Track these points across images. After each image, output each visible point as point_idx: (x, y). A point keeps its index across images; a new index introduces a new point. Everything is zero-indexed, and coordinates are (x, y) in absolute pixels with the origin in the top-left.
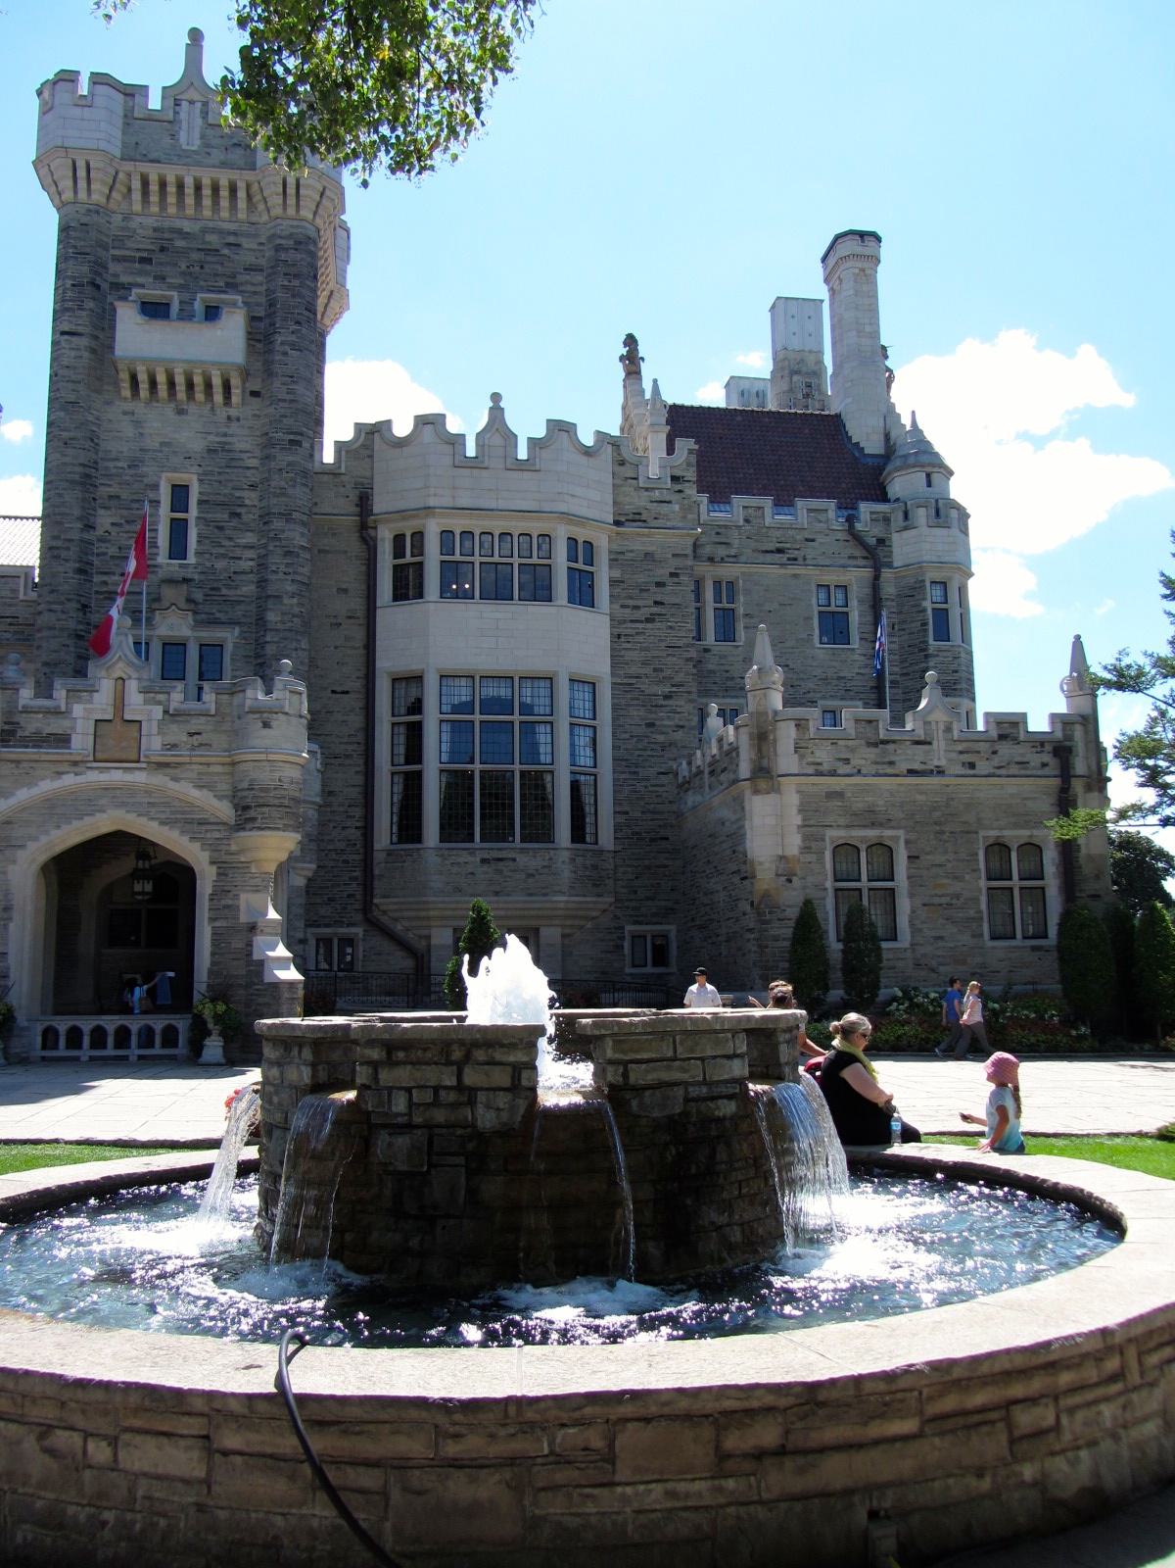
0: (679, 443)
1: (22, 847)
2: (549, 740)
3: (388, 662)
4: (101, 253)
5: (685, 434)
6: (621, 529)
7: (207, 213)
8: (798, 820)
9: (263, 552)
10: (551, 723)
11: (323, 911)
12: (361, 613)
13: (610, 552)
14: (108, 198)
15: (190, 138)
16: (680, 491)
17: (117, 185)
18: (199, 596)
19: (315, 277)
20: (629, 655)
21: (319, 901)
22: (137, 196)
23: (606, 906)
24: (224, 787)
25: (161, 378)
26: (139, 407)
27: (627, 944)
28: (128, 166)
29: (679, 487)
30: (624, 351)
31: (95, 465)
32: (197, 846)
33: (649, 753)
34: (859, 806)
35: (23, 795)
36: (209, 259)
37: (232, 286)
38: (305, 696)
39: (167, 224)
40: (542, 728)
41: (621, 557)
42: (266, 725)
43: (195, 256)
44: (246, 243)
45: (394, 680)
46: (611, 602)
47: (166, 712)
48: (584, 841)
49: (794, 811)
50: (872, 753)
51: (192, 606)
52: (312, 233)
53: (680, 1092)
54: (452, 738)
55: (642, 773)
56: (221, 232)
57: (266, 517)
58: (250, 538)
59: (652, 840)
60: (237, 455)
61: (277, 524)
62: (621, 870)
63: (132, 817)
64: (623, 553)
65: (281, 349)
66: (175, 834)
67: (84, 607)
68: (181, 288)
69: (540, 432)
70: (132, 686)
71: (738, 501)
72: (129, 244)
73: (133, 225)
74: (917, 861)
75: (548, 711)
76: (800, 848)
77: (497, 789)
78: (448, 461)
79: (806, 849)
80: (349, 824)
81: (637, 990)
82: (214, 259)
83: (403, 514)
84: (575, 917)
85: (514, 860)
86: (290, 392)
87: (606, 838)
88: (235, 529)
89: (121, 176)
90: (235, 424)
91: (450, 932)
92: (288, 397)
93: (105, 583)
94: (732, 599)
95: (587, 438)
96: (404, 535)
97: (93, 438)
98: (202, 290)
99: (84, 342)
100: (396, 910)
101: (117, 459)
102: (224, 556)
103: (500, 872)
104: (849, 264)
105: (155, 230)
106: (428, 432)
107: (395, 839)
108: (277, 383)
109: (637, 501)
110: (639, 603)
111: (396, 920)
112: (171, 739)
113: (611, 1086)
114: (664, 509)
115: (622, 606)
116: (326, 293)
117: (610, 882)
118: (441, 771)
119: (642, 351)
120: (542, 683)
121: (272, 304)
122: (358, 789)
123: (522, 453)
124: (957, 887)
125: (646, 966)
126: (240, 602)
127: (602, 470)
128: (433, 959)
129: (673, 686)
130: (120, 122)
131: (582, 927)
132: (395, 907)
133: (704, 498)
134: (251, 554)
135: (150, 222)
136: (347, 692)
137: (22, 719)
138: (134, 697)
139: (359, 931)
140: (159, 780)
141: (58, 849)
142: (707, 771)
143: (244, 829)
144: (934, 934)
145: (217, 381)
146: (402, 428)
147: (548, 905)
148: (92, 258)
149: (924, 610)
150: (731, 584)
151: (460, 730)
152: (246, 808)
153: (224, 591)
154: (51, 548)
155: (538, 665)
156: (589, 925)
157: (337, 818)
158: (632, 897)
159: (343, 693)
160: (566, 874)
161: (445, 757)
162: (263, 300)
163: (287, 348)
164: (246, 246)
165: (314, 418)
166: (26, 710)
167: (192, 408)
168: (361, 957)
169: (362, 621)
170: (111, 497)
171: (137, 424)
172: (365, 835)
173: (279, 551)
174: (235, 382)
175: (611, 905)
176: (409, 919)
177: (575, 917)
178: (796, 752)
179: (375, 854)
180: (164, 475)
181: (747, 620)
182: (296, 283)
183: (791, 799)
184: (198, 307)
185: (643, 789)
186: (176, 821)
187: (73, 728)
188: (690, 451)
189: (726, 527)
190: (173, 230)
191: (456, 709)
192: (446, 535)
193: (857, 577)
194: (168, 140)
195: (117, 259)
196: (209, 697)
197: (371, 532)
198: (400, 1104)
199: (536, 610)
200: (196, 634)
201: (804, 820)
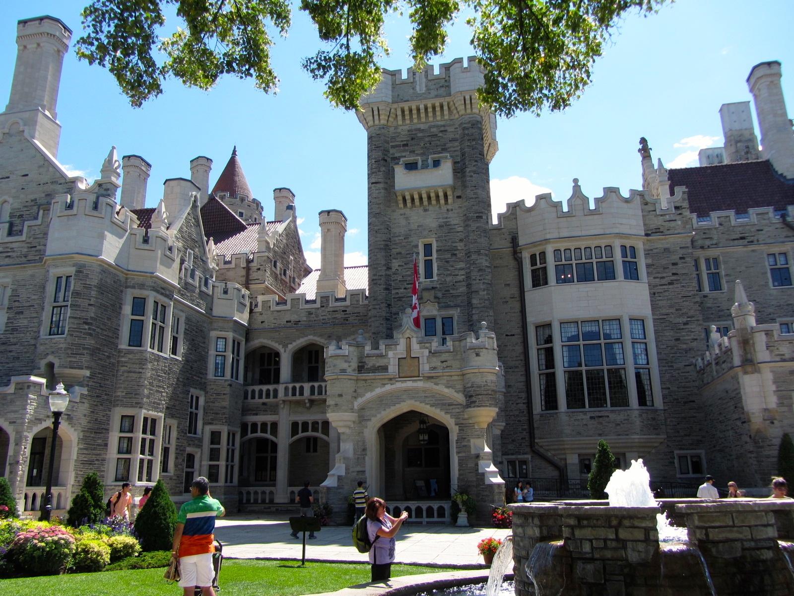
0: (677, 189)
1: (370, 420)
2: (621, 352)
3: (533, 318)
4: (386, 145)
5: (680, 184)
7: (431, 119)
8: (774, 388)
9: (468, 271)
11: (510, 447)
13: (645, 250)
15: (421, 88)
16: (680, 214)
18: (440, 295)
19: (482, 139)
20: (660, 303)
22: (400, 118)
23: (662, 440)
24: (459, 386)
25: (416, 197)
26: (407, 211)
27: (676, 461)
28: (395, 106)
30: (640, 146)
32: (448, 416)
33: (678, 355)
35: (369, 395)
36: (433, 139)
37: (444, 150)
38: (495, 339)
39: (414, 127)
40: (616, 346)
41: (650, 252)
42: (478, 355)
43: (427, 139)
44: (450, 129)
45: (537, 327)
46: (648, 277)
47: (430, 352)
48: (646, 405)
49: (770, 382)
51: (437, 300)
52: (479, 119)
53: (739, 545)
54: (569, 354)
55: (676, 366)
56: (437, 126)
57: (468, 254)
58: (462, 265)
59: (685, 403)
60: (453, 227)
61: (474, 257)
62: (669, 420)
63: (417, 403)
65: (469, 175)
67: (389, 305)
68: (422, 154)
69: (600, 194)
70: (414, 341)
71: (714, 215)
72: (398, 139)
73: (399, 130)
75: (619, 337)
77: (595, 379)
78: (554, 215)
79: (781, 404)
80: (519, 401)
81: (685, 487)
82: (436, 139)
83: (534, 244)
85: (608, 416)
87: (659, 403)
89: (392, 110)
91: (576, 456)
92: (474, 196)
93: (397, 293)
94: (717, 267)
95: (625, 194)
96: (535, 255)
97: (388, 228)
98: (431, 154)
99: (381, 186)
100: (548, 446)
101: (400, 236)
102: (450, 275)
103: (601, 423)
104: (763, 80)
105: (409, 131)
106: (543, 201)
107: (543, 408)
108: (468, 191)
109: (657, 222)
110: (664, 275)
111: (548, 450)
112: (433, 365)
113: (700, 541)
114: (672, 224)
115: (655, 278)
116: (487, 145)
120: (614, 322)
121: (463, 155)
122: (522, 384)
123: (592, 206)
125: (689, 473)
127: (636, 208)
128: (569, 471)
129: (688, 317)
130: (390, 88)
131: (649, 452)
132: (547, 444)
133: (694, 215)
134: (463, 272)
135: (407, 128)
137: (366, 360)
138: (415, 346)
139: (529, 457)
140: (429, 385)
141: (386, 420)
142: (714, 363)
143: (470, 407)
145: (441, 194)
146: (529, 203)
147: (629, 441)
148: (382, 148)
150: (715, 260)
151: (573, 350)
152: (471, 396)
153: (451, 292)
154: (373, 280)
156: (653, 451)
159: (511, 335)
160: (638, 422)
161: (566, 365)
162: (459, 153)
163: (472, 174)
164: (449, 130)
165: (487, 204)
166: (368, 356)
167: (431, 208)
168: (531, 470)
169: (518, 299)
170: (397, 254)
171: (407, 219)
172: (528, 407)
173: (476, 270)
174: (449, 193)
176: (555, 450)
178: (767, 349)
179: (534, 416)
180: (420, 240)
181: (728, 278)
182: (474, 143)
184: (430, 161)
185: (677, 375)
186: (438, 404)
187: (389, 363)
188: (684, 193)
189: (708, 229)
191: (570, 339)
192: (557, 251)
195: (393, 147)
196: (449, 343)
197: (519, 255)
198: (587, 548)
199: (608, 284)
201: (777, 387)
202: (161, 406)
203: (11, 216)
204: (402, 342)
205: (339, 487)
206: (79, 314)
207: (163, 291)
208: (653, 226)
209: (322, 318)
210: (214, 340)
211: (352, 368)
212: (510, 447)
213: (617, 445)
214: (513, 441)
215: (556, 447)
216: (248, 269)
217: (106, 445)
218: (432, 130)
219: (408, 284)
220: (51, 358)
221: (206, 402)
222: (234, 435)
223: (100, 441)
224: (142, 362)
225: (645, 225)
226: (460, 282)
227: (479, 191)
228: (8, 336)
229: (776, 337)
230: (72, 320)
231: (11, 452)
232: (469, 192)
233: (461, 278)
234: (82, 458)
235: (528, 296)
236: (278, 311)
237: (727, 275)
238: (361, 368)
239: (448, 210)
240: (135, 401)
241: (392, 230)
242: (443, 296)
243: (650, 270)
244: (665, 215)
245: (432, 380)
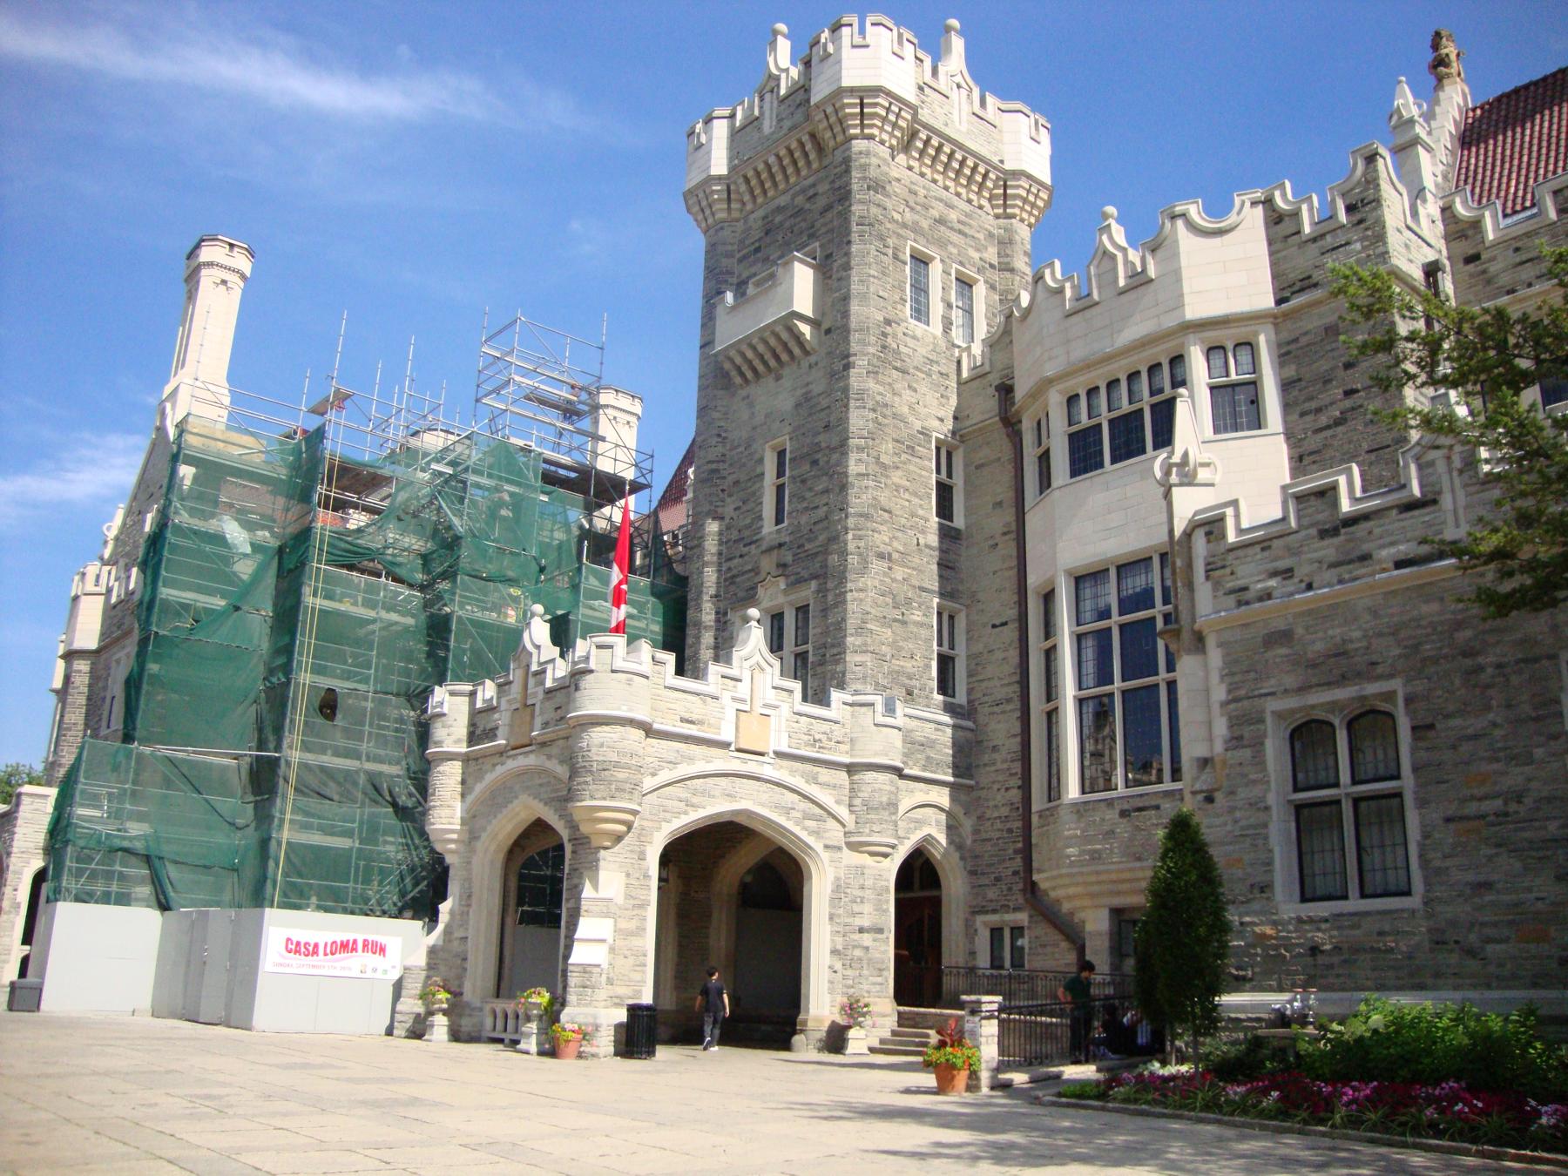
3: (1032, 580)
8: (1219, 693)
11: (992, 894)
12: (1014, 527)
13: (1279, 345)
14: (729, 208)
15: (767, 126)
16: (1360, 222)
17: (733, 196)
18: (789, 558)
21: (987, 882)
22: (747, 198)
25: (750, 354)
29: (1358, 216)
37: (812, 236)
41: (1292, 347)
49: (1215, 678)
50: (1329, 549)
64: (1296, 340)
74: (1431, 734)
76: (1226, 742)
79: (1235, 742)
89: (732, 187)
90: (813, 370)
101: (739, 446)
102: (806, 509)
105: (764, 218)
115: (1302, 415)
124: (1515, 777)
126: (816, 554)
135: (760, 213)
136: (1004, 624)
139: (1022, 918)
144: (1470, 877)
145: (785, 336)
157: (1000, 778)
161: (1090, 680)
164: (820, 191)
167: (786, 372)
169: (1013, 536)
178: (1207, 578)
183: (1215, 657)
189: (1528, 235)
192: (1072, 400)
195: (740, 261)
200: (793, 597)
201: (1229, 692)
208: (1293, 276)
212: (992, 894)
214: (998, 879)
219: (745, 546)
226: (821, 521)
233: (821, 512)
235: (1033, 522)
238: (473, 738)
244: (1322, 236)
245: (547, 750)
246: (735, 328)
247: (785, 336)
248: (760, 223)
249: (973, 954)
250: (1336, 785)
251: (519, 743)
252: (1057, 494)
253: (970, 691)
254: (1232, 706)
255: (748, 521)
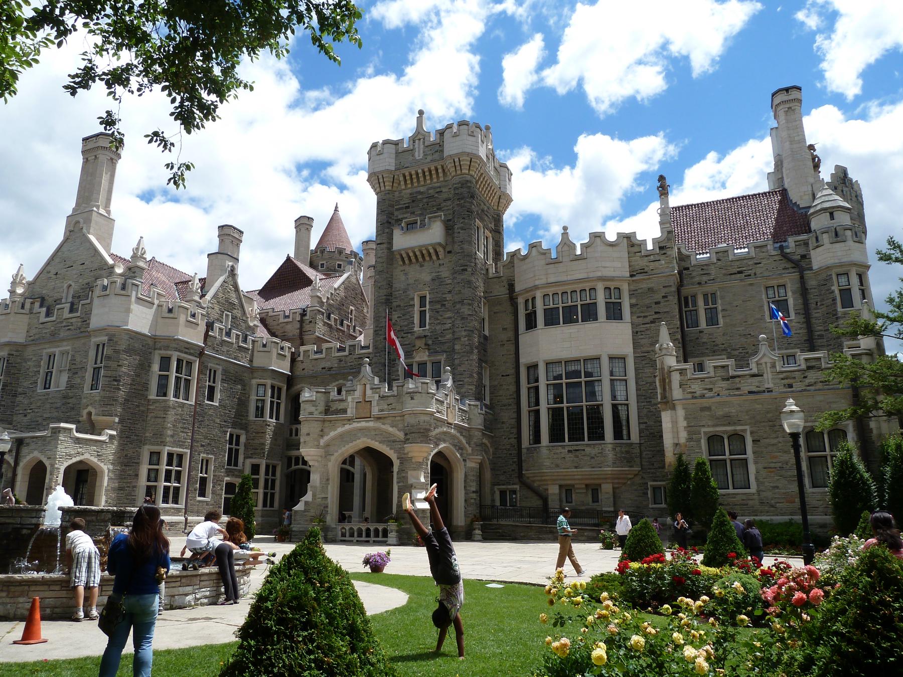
1: (333, 455)
3: (524, 360)
6: (634, 278)
7: (428, 182)
8: (685, 424)
10: (626, 380)
11: (502, 478)
12: (513, 338)
15: (419, 155)
16: (664, 254)
18: (430, 342)
20: (643, 342)
22: (402, 183)
23: (637, 472)
26: (406, 268)
29: (664, 252)
30: (659, 184)
31: (391, 295)
34: (720, 413)
35: (332, 434)
37: (439, 209)
39: (415, 190)
40: (596, 384)
42: (412, 398)
44: (444, 190)
46: (631, 316)
50: (725, 384)
52: (469, 178)
58: (449, 314)
61: (458, 306)
62: (644, 453)
63: (369, 441)
66: (384, 447)
70: (368, 387)
73: (402, 194)
78: (543, 262)
79: (690, 439)
80: (511, 436)
83: (527, 291)
84: (618, 478)
85: (584, 450)
86: (462, 248)
87: (635, 437)
88: (443, 311)
91: (557, 487)
92: (460, 251)
94: (714, 302)
99: (385, 246)
102: (439, 323)
104: (781, 107)
105: (411, 194)
108: (456, 246)
109: (641, 263)
112: (381, 407)
115: (638, 317)
117: (638, 460)
118: (548, 409)
119: (668, 182)
122: (514, 420)
123: (578, 252)
127: (623, 252)
128: (550, 500)
135: (409, 191)
137: (331, 404)
139: (517, 487)
140: (378, 425)
145: (432, 251)
149: (833, 292)
153: (440, 339)
155: (591, 352)
158: (651, 467)
160: (610, 456)
161: (551, 401)
162: (451, 212)
164: (444, 191)
166: (333, 401)
167: (426, 264)
169: (514, 342)
171: (406, 274)
175: (639, 471)
177: (618, 478)
183: (681, 413)
189: (706, 265)
190: (417, 192)
191: (555, 378)
192: (545, 296)
193: (790, 280)
194: (411, 158)
195: (397, 210)
196: (395, 389)
197: (516, 300)
199: (590, 326)
201: (688, 423)
202: (186, 444)
203: (73, 297)
204: (359, 388)
205: (305, 511)
206: (109, 373)
207: (187, 350)
208: (637, 267)
209: (349, 364)
210: (255, 387)
211: (319, 411)
212: (502, 478)
213: (592, 477)
215: (539, 478)
216: (302, 322)
217: (137, 475)
218: (430, 191)
220: (90, 409)
221: (247, 439)
222: (274, 467)
223: (131, 472)
224: (166, 409)
225: (630, 266)
227: (466, 246)
228: (69, 391)
229: (689, 376)
230: (105, 378)
231: (47, 481)
232: (457, 248)
233: (448, 326)
234: (113, 485)
235: (522, 339)
236: (316, 359)
237: (723, 310)
238: (327, 411)
239: (440, 265)
240: (160, 440)
241: (394, 286)
242: (433, 343)
243: (635, 309)
245: (381, 420)
246: (402, 241)
247: (432, 251)
248: (408, 196)
249: (493, 501)
250: (725, 455)
251: (358, 417)
252: (540, 331)
253: (491, 400)
254: (689, 429)
255: (406, 323)
